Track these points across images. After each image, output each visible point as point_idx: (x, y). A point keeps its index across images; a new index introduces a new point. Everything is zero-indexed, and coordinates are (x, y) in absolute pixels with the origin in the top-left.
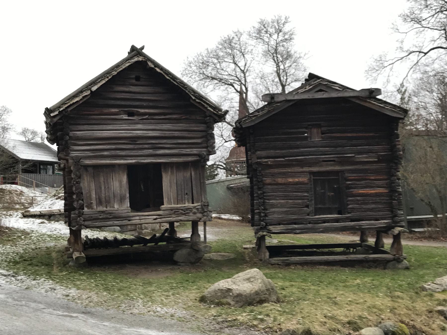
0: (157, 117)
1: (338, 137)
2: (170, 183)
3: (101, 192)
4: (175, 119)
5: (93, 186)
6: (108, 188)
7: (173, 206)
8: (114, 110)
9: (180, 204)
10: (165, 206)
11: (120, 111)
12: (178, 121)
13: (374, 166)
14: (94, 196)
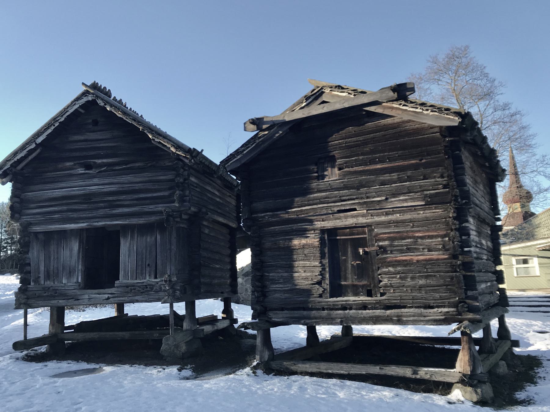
0: (117, 168)
1: (361, 171)
2: (129, 251)
3: (50, 262)
4: (139, 168)
5: (42, 258)
6: (58, 258)
7: (130, 281)
8: (68, 164)
9: (140, 279)
10: (122, 280)
11: (75, 165)
12: (141, 170)
13: (422, 214)
14: (42, 268)
